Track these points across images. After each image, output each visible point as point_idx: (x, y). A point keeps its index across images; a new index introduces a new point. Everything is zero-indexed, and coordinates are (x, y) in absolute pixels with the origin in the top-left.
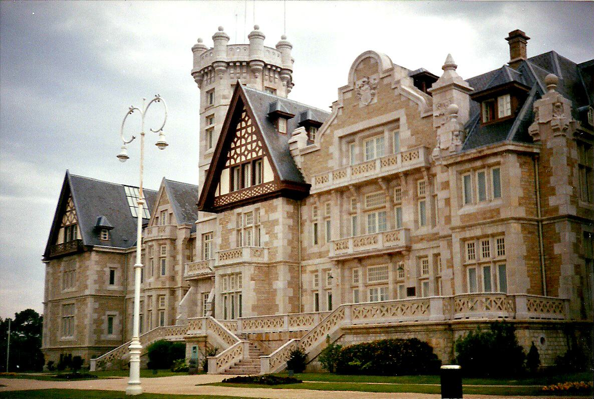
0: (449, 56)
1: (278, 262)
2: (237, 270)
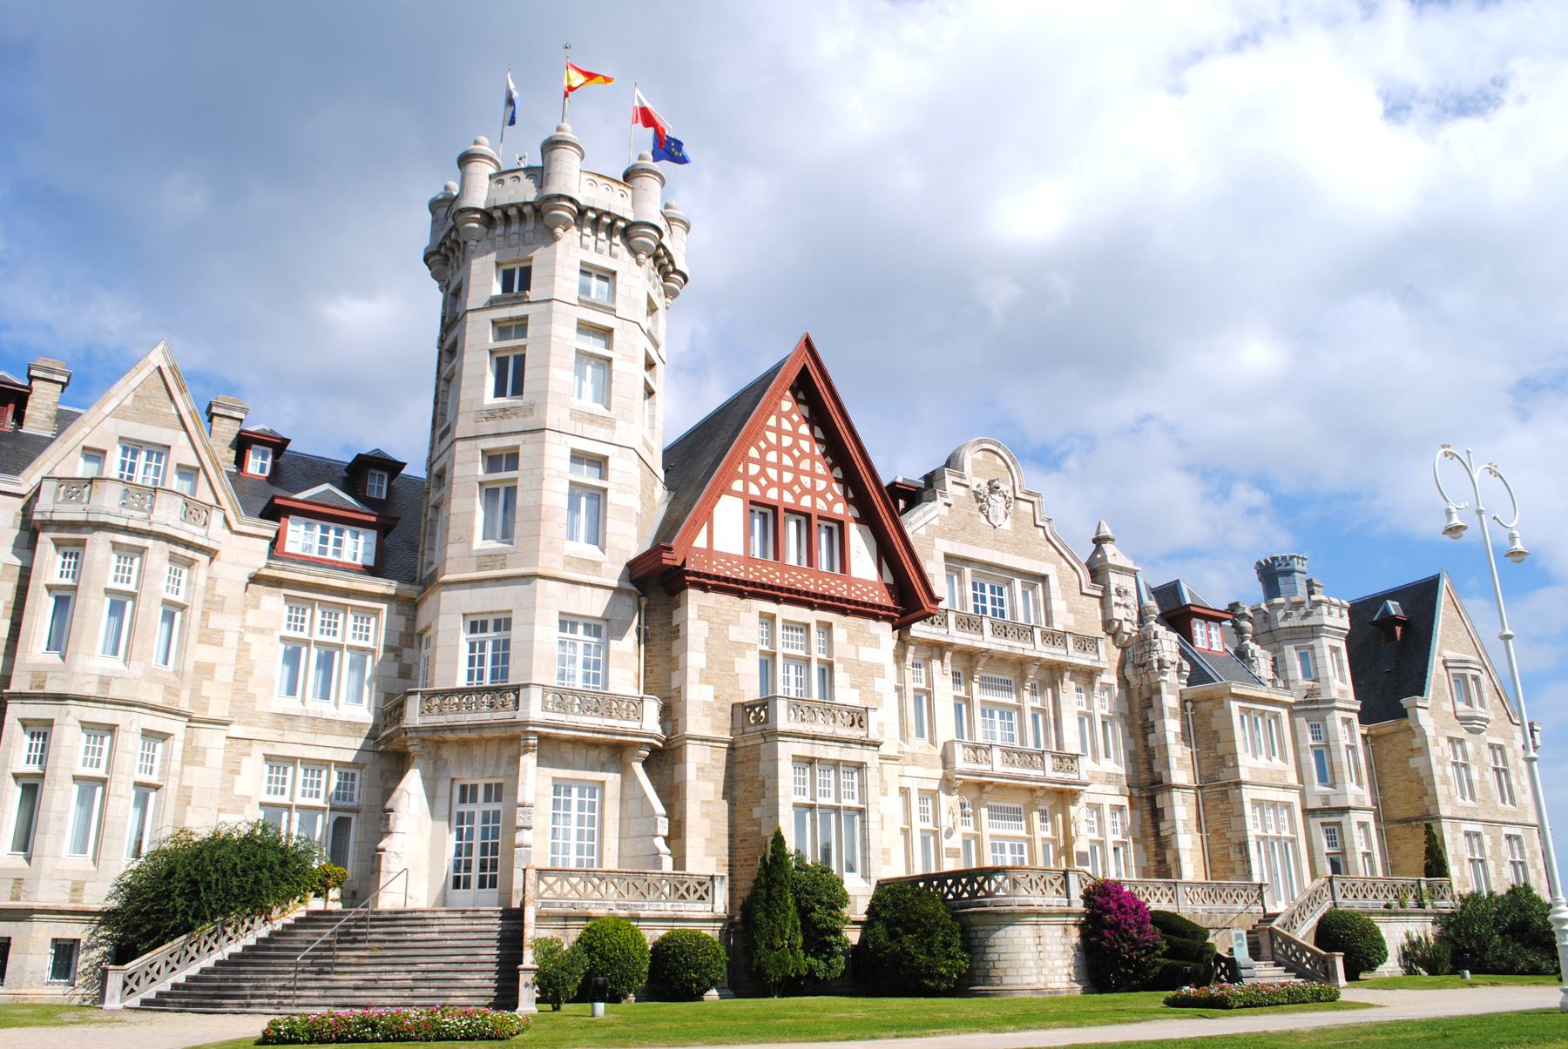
2: (854, 754)
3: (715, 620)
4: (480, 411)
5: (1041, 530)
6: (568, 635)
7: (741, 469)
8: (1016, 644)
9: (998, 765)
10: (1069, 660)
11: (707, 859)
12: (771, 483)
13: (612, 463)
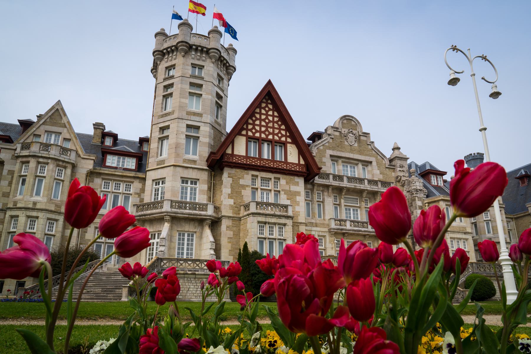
0: (395, 143)
1: (301, 223)
3: (235, 178)
4: (160, 116)
5: (369, 146)
6: (185, 185)
7: (245, 126)
8: (357, 185)
9: (348, 226)
10: (379, 190)
11: (230, 257)
12: (257, 131)
13: (201, 128)
